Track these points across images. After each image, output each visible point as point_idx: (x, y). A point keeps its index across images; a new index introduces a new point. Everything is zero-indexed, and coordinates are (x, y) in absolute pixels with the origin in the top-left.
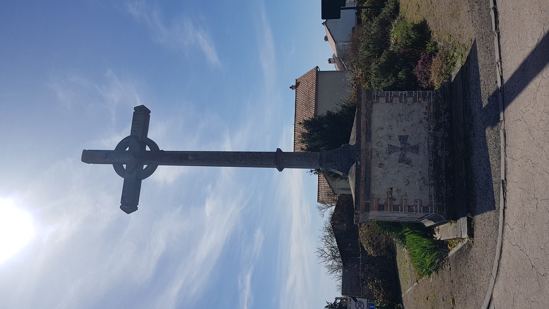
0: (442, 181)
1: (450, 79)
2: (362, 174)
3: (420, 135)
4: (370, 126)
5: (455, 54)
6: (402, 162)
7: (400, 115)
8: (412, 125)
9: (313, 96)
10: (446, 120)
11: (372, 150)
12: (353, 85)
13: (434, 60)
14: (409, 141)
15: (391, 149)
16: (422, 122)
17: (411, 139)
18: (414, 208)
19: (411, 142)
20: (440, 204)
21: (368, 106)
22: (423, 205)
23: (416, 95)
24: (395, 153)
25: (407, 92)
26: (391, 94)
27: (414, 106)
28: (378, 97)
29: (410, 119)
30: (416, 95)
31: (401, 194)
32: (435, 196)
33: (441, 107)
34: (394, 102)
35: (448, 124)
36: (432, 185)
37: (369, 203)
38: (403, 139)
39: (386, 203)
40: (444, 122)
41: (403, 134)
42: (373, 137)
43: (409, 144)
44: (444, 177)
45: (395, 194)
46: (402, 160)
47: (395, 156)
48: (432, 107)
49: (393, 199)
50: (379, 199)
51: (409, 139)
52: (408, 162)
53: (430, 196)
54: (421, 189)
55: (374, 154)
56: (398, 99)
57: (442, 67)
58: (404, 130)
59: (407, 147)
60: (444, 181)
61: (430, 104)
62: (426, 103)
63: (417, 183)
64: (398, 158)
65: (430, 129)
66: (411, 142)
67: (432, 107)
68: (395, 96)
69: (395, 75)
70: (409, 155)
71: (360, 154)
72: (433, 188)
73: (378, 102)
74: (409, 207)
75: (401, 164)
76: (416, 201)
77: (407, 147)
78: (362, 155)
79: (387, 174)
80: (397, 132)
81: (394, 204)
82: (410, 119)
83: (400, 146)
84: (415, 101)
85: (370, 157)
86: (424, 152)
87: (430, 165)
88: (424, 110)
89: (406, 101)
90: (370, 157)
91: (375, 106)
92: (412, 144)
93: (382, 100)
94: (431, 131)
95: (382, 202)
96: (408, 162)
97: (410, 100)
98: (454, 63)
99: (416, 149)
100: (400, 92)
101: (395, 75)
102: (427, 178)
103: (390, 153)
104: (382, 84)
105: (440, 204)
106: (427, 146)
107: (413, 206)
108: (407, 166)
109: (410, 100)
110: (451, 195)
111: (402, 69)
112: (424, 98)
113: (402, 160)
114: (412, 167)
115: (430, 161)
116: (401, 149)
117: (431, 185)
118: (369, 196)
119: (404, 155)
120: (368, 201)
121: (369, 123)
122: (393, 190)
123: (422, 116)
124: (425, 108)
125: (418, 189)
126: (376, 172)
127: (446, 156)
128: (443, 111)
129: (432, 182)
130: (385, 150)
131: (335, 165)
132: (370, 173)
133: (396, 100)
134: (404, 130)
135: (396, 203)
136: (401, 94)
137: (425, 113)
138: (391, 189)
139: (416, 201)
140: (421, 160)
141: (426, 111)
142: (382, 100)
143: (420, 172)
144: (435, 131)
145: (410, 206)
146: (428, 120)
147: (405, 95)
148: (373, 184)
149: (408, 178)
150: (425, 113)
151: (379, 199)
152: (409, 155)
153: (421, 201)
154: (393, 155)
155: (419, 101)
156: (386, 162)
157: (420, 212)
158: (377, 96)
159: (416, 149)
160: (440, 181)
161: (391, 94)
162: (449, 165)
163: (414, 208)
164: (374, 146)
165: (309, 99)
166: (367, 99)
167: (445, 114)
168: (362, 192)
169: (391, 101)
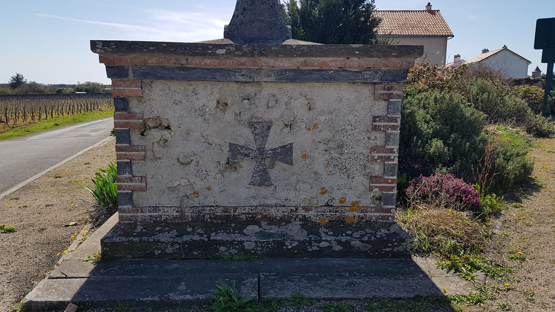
0: (188, 233)
1: (420, 252)
2: (195, 61)
3: (295, 191)
4: (317, 80)
5: (479, 275)
6: (230, 150)
7: (341, 146)
8: (316, 173)
9: (416, 32)
10: (323, 244)
11: (259, 83)
12: (425, 66)
13: (464, 214)
14: (280, 165)
15: (261, 128)
16: (323, 193)
17: (285, 170)
18: (127, 175)
19: (278, 172)
20: (139, 229)
21: (367, 75)
22: (135, 196)
23: (386, 181)
24: (252, 137)
25: (396, 162)
26: (394, 128)
27: (362, 178)
28: (387, 98)
29: (331, 169)
30: (386, 181)
31: (156, 148)
32: (156, 217)
33: (356, 235)
34: (374, 134)
35: (314, 248)
36: (182, 212)
37: (127, 76)
38: (285, 153)
39: (132, 116)
40: (319, 241)
41: (296, 154)
42: (290, 88)
43: (273, 166)
44: (196, 238)
45: (155, 135)
46: (236, 153)
47: (245, 136)
48: (357, 214)
49: (144, 130)
50: (140, 98)
51: (285, 165)
52: (231, 164)
53: (156, 208)
54: (172, 189)
55: (250, 89)
56: (380, 142)
57: (448, 234)
58: (304, 156)
59: (267, 162)
60: (186, 238)
61: (364, 210)
62: (366, 202)
63: (184, 182)
64: (241, 142)
65: (306, 209)
66: (278, 172)
67: (357, 214)
68: (388, 137)
69: (436, 134)
70: (247, 167)
71: (244, 55)
72: (175, 214)
73: (376, 98)
74: (129, 165)
75: (226, 149)
76: (143, 179)
77: (267, 162)
78: (243, 60)
79: (200, 119)
80: (301, 140)
81: (132, 133)
82: (331, 169)
83: (268, 147)
84: (373, 179)
85: (241, 79)
86: (254, 198)
87: (226, 209)
88: (351, 198)
89: (374, 160)
90: (241, 79)
91: (366, 91)
92: (273, 173)
93: (380, 108)
94: (301, 212)
95: (135, 106)
96: (231, 164)
97: (377, 169)
98: (457, 270)
99: (263, 179)
100: (396, 148)
101: (436, 134)
102: (196, 202)
103: (251, 125)
104: (421, 111)
105: (139, 229)
106: (268, 202)
107: (131, 172)
108: (223, 162)
109: (377, 169)
110: (157, 252)
111: (449, 146)
112: (379, 199)
113: (236, 153)
114: (221, 172)
115: (236, 209)
116: (261, 151)
117: (181, 210)
118: (145, 75)
119: (247, 156)
120: (131, 75)
121: (324, 77)
122: (166, 133)
123: (338, 195)
124: (355, 199)
125: (170, 185)
126: (206, 94)
127: (242, 242)
128: (344, 239)
129: (188, 213)
130: (259, 115)
131: (245, 9)
132: (203, 79)
133: (379, 138)
134: (304, 156)
135: (135, 138)
136: (391, 151)
137: (342, 201)
138: (168, 128)
139: (143, 179)
140: (236, 192)
141: (348, 203)
142: (380, 108)
143: (209, 189)
144: (300, 220)
145: (131, 167)
146: (327, 205)
147: (389, 159)
148: (175, 86)
149: (194, 163)
150: (342, 201)
151: (140, 98)
152: (247, 167)
153: (145, 189)
154: (247, 132)
155: (371, 189)
156: (229, 116)
157: (120, 188)
158: (390, 96)
159: (263, 179)
160: (189, 229)
161: (394, 128)
162: (222, 248)
163: (127, 175)
164: (268, 90)
165: (413, 27)
166: (385, 73)
167: (339, 242)
168: (152, 60)
169: (375, 128)
